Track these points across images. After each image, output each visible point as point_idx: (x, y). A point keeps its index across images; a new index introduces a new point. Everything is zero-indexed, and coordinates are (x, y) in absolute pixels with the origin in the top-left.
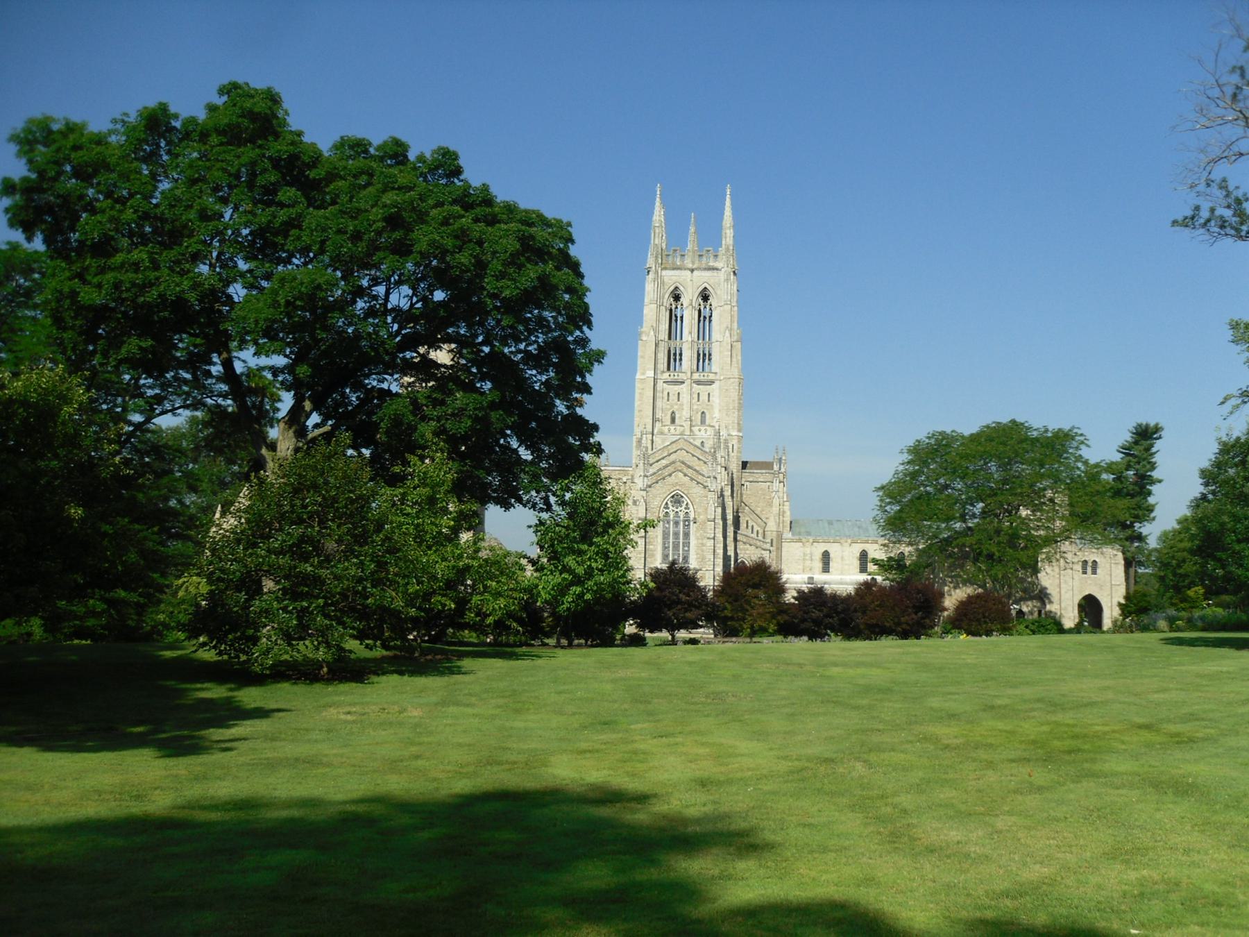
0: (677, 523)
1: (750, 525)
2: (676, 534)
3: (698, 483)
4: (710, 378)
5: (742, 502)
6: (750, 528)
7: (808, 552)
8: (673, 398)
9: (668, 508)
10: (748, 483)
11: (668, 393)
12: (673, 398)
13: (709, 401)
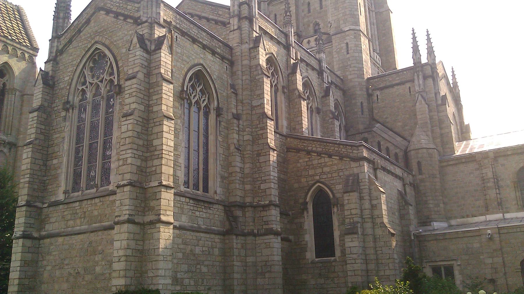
0: (96, 107)
2: (94, 127)
3: (126, 17)
5: (373, 120)
7: (490, 175)
9: (84, 83)
10: (378, 93)
11: (276, 15)
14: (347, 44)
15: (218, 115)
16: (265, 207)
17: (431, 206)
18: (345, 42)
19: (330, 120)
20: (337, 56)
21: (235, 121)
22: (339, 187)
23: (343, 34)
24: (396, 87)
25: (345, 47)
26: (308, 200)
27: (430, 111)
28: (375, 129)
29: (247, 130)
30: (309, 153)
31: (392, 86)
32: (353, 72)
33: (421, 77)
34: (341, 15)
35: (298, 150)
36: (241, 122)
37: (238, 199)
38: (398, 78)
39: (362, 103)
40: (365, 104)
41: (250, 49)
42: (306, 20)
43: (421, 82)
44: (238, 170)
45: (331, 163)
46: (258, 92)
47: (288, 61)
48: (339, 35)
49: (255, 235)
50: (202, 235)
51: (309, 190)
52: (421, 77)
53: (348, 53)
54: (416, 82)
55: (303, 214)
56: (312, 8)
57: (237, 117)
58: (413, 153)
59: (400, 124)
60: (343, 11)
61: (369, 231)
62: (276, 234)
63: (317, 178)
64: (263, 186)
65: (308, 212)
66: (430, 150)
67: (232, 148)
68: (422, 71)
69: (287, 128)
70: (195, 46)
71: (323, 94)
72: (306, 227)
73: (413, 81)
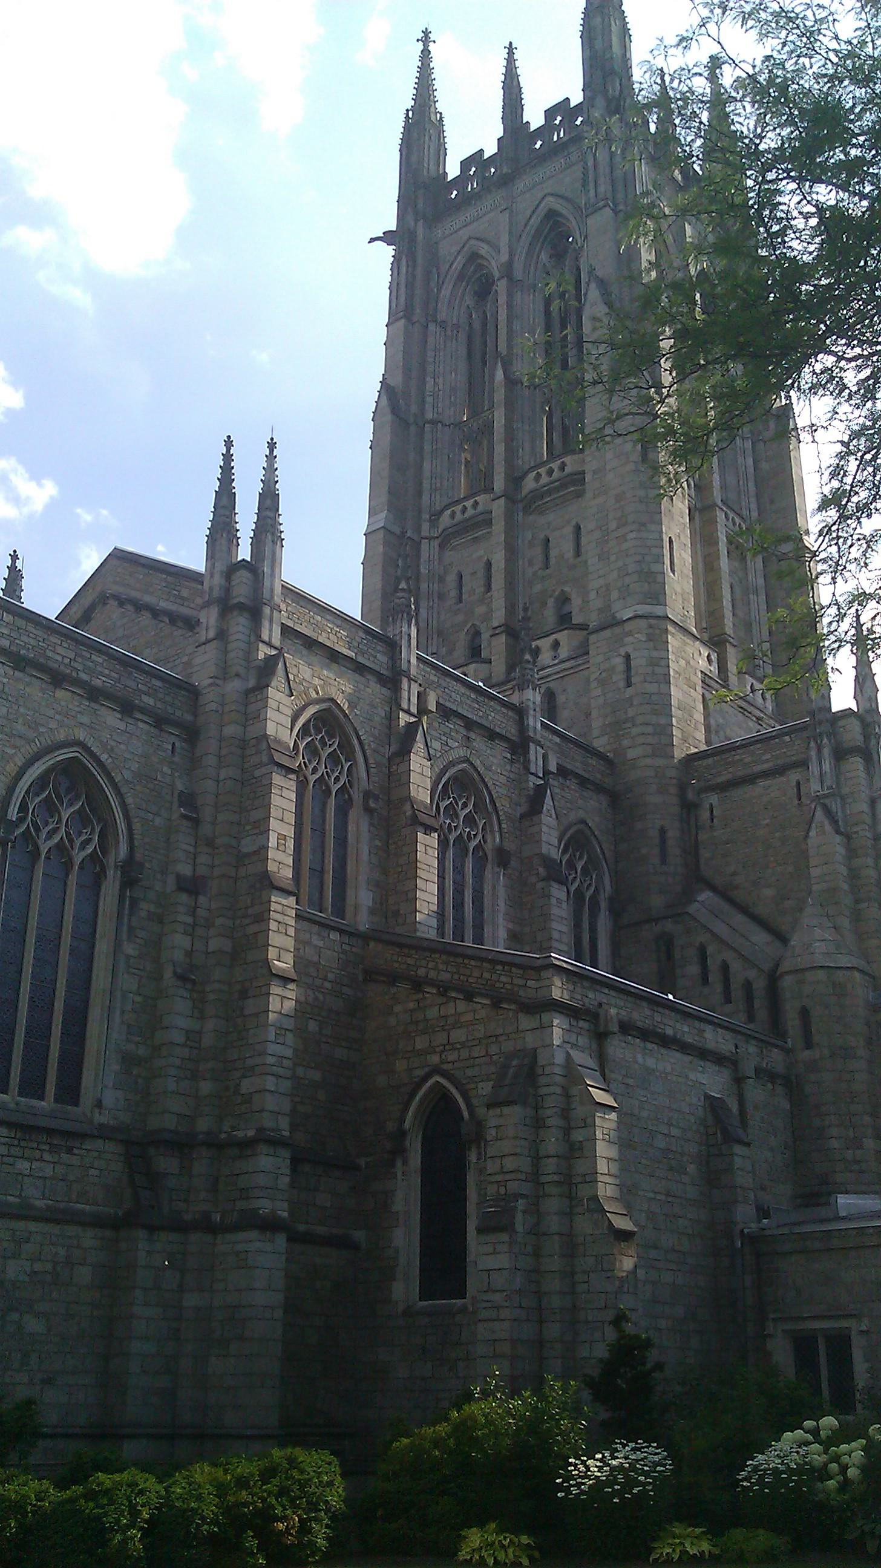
1: (713, 964)
4: (568, 470)
6: (715, 977)
8: (473, 584)
10: (714, 799)
12: (473, 584)
13: (578, 552)
14: (628, 657)
15: (129, 881)
16: (247, 1146)
17: (835, 1144)
18: (622, 651)
19: (540, 885)
20: (599, 692)
21: (184, 897)
22: (485, 1088)
23: (617, 630)
24: (762, 783)
25: (621, 668)
26: (407, 1124)
27: (852, 852)
28: (692, 908)
29: (219, 921)
30: (417, 985)
31: (750, 780)
32: (641, 740)
33: (826, 752)
34: (615, 574)
35: (393, 978)
36: (202, 899)
37: (169, 1122)
38: (768, 756)
39: (663, 831)
40: (673, 834)
41: (248, 692)
42: (538, 588)
43: (827, 767)
44: (178, 1037)
45: (469, 1017)
46: (256, 815)
47: (391, 718)
48: (607, 633)
49: (213, 1229)
50: (32, 1226)
51: (412, 1095)
52: (826, 752)
53: (629, 685)
54: (814, 768)
55: (393, 1166)
56: (553, 553)
57: (192, 886)
58: (787, 982)
59: (769, 892)
60: (620, 564)
61: (554, 1223)
62: (269, 1225)
63: (435, 1059)
64: (246, 1086)
65: (405, 1162)
66: (840, 973)
67: (168, 974)
68: (832, 734)
69: (372, 912)
70: (60, 694)
71: (523, 808)
72: (398, 1206)
73: (804, 764)
